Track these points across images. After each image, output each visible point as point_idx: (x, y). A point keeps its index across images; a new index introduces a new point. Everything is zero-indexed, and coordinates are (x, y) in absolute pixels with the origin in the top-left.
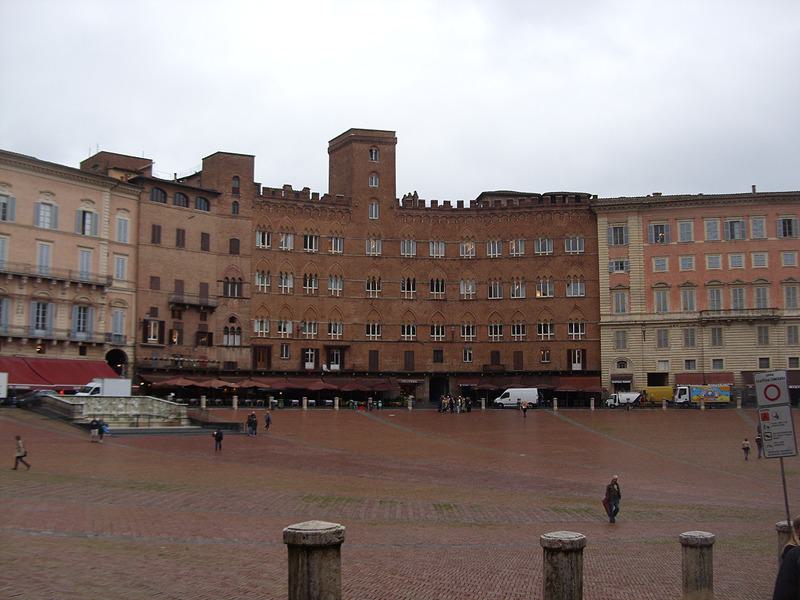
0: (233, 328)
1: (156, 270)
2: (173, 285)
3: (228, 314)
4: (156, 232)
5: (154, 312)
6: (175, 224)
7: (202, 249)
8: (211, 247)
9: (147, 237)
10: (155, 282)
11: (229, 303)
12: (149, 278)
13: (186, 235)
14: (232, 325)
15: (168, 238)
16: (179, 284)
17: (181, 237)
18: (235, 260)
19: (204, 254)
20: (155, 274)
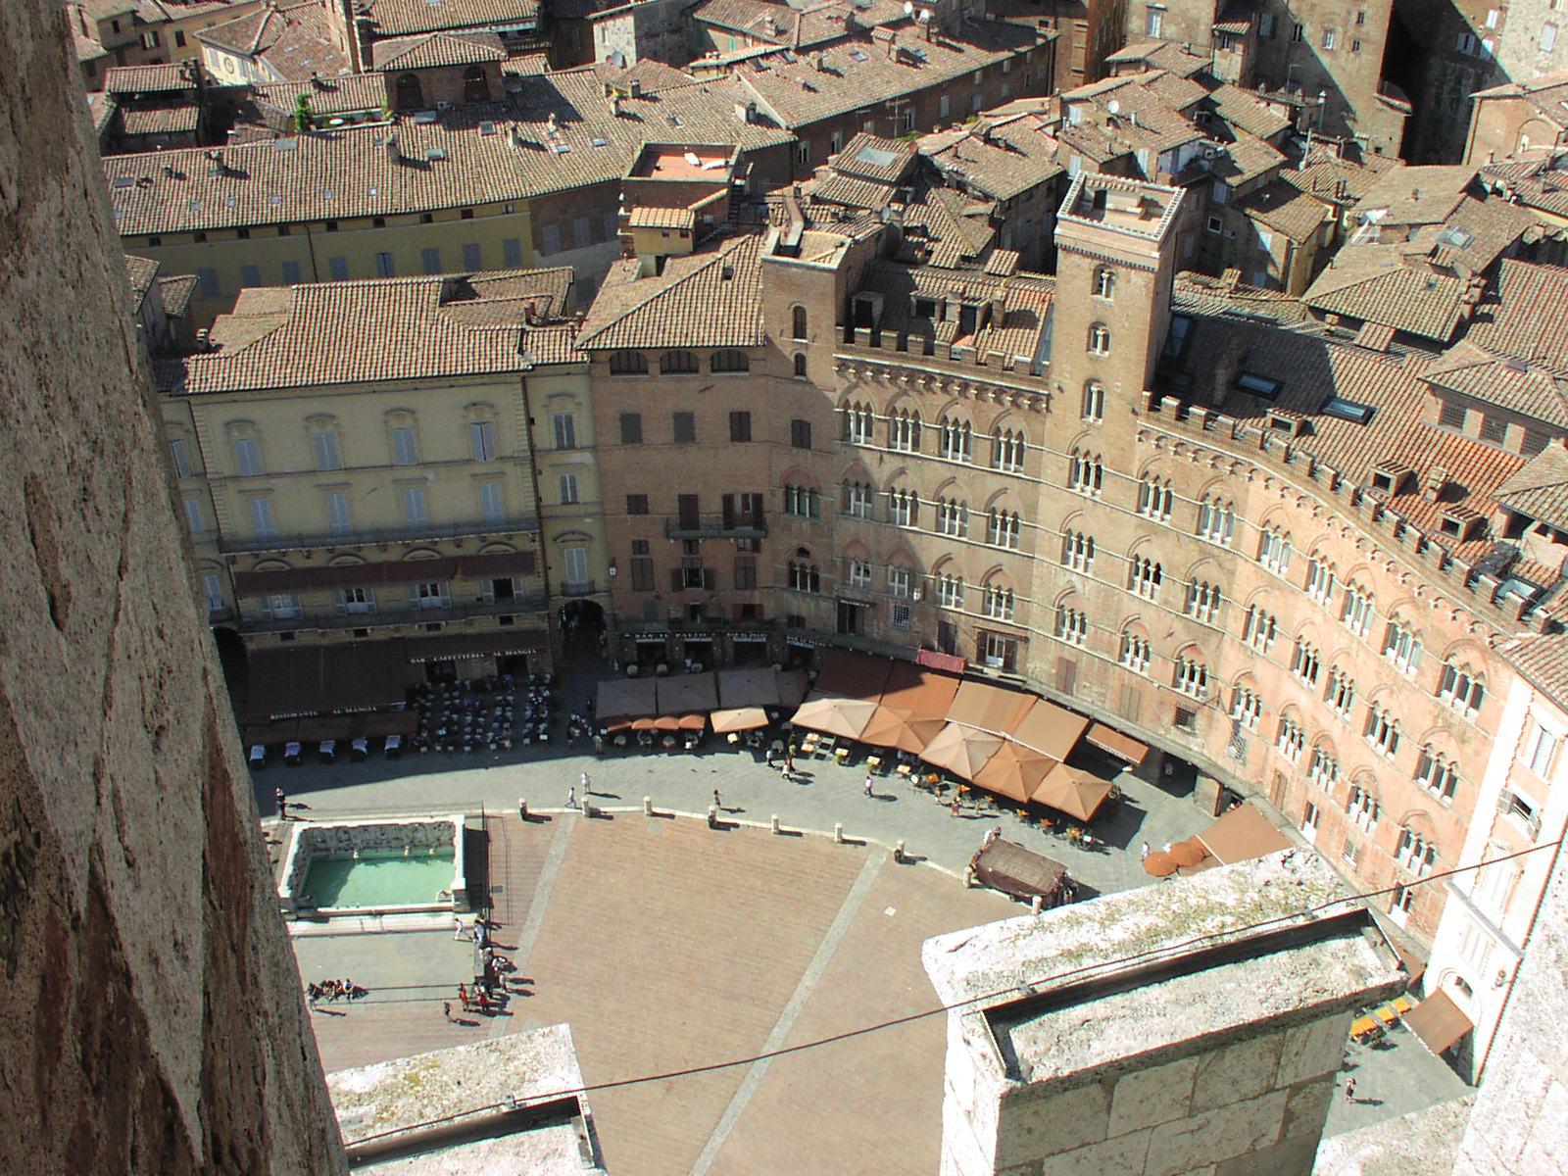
0: (803, 566)
1: (636, 485)
2: (677, 504)
3: (795, 543)
4: (631, 428)
5: (640, 546)
6: (671, 406)
7: (733, 439)
8: (754, 433)
9: (613, 434)
10: (637, 504)
11: (795, 526)
12: (625, 500)
13: (697, 422)
14: (804, 560)
15: (657, 430)
16: (689, 505)
17: (685, 427)
18: (803, 458)
19: (741, 446)
20: (635, 491)
